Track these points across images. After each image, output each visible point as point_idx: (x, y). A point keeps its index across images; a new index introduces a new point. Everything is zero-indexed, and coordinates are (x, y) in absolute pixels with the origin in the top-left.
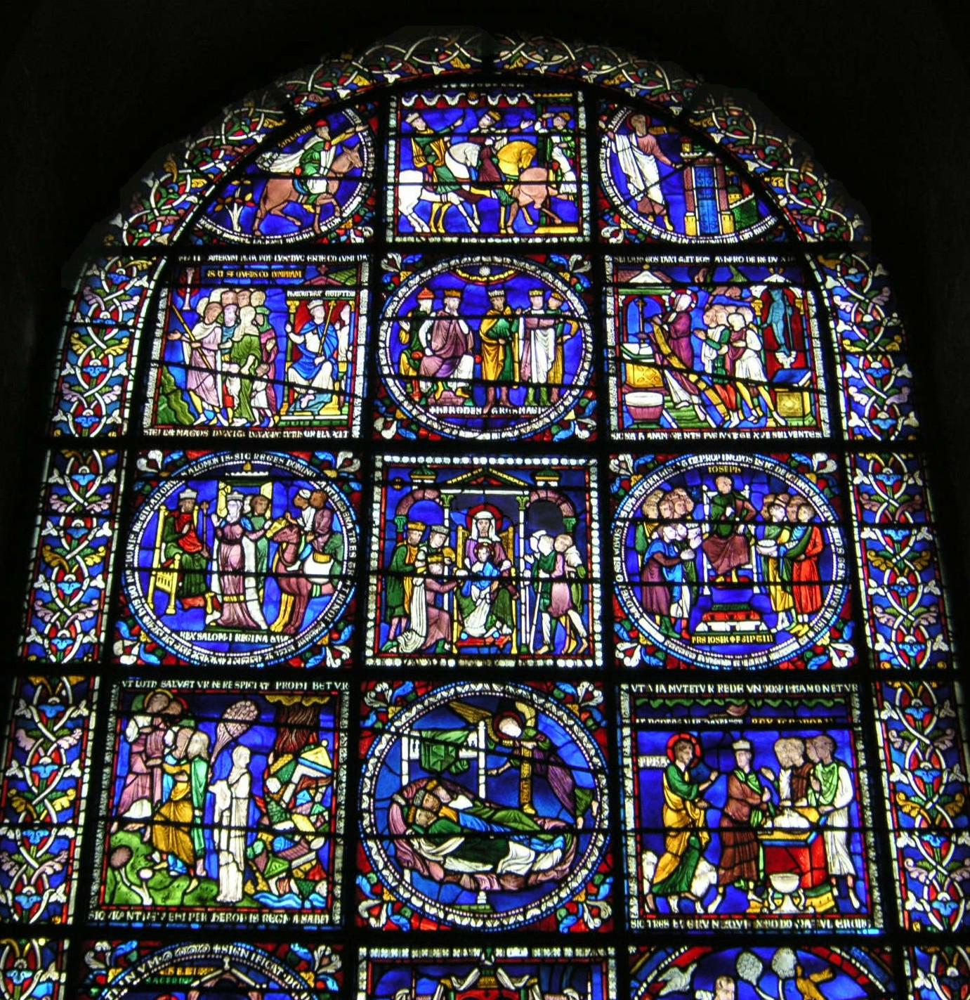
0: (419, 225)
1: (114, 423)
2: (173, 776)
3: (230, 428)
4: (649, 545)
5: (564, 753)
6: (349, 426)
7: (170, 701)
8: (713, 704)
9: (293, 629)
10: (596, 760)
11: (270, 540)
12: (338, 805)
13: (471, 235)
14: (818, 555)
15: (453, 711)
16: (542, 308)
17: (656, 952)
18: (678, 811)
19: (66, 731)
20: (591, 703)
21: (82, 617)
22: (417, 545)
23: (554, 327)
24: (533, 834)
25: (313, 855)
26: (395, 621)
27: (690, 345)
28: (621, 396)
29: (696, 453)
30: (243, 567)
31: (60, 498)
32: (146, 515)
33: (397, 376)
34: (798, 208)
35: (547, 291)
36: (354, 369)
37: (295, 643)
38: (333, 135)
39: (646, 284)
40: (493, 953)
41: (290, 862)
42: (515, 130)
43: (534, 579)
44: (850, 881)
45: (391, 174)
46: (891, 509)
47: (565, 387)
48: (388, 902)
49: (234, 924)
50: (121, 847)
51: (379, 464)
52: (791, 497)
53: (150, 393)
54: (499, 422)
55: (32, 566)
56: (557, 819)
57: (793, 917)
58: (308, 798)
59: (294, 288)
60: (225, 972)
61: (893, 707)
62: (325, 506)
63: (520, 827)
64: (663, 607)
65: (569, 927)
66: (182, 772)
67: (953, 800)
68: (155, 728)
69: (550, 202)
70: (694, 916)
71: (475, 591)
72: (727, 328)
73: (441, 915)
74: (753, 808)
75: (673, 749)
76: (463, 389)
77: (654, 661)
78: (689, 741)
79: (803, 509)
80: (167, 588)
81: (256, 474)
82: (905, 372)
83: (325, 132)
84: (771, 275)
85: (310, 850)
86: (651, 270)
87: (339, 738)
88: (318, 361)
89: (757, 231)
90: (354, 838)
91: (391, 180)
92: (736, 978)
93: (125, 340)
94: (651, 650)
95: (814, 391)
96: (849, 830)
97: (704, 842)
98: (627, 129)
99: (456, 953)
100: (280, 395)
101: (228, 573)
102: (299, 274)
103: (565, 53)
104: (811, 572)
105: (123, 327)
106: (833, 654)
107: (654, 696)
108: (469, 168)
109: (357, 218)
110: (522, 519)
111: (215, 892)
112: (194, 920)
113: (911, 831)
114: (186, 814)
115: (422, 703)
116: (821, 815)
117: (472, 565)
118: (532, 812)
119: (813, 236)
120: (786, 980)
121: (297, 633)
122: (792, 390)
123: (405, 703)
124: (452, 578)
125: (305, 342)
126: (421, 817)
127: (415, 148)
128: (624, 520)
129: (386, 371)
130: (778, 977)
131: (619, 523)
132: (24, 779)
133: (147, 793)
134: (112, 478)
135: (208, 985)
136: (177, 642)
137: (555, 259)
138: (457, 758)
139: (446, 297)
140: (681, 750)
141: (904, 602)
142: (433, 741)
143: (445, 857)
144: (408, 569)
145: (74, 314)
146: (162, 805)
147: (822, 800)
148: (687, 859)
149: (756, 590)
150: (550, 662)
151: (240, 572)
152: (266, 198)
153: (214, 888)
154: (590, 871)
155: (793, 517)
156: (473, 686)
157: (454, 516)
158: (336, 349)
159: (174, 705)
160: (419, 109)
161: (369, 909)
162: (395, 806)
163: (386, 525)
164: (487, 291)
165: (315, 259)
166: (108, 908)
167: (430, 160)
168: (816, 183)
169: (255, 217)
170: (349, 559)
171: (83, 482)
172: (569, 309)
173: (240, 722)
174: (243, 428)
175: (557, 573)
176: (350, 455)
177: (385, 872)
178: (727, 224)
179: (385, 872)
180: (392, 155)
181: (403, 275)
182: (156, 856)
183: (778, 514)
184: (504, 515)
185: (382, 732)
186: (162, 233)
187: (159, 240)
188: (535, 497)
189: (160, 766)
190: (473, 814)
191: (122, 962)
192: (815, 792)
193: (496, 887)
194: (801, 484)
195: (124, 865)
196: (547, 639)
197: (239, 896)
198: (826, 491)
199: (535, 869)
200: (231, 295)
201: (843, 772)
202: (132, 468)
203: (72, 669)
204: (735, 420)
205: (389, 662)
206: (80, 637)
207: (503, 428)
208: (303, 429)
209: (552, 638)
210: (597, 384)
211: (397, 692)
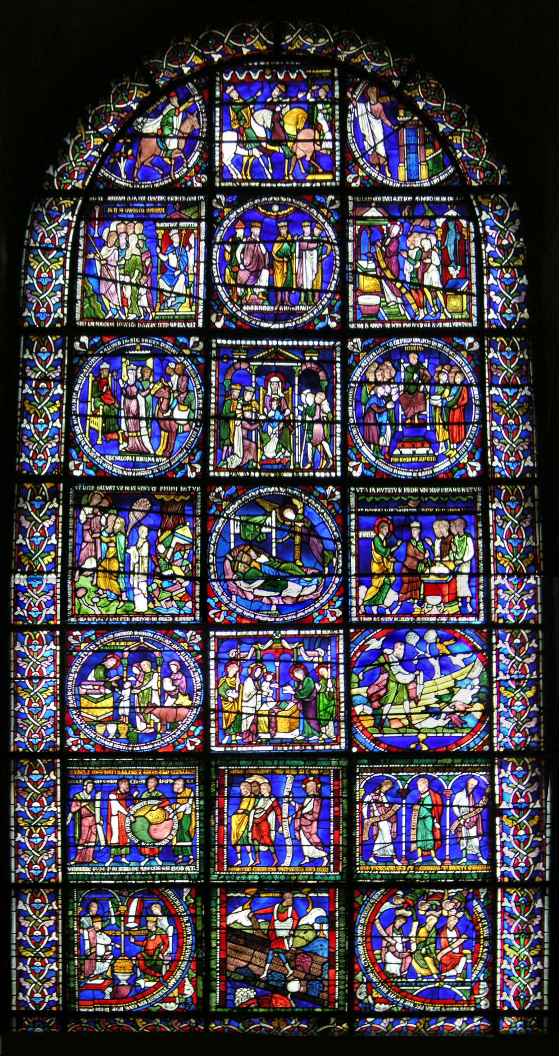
0: (236, 174)
1: (58, 318)
2: (107, 543)
3: (127, 321)
4: (369, 399)
5: (319, 529)
6: (196, 320)
8: (401, 499)
9: (168, 454)
10: (336, 533)
11: (153, 396)
12: (197, 560)
13: (267, 181)
14: (465, 405)
15: (258, 504)
16: (310, 235)
18: (379, 564)
19: (46, 517)
21: (50, 446)
22: (237, 400)
23: (317, 248)
26: (225, 448)
27: (398, 261)
28: (356, 297)
29: (398, 337)
30: (139, 414)
31: (31, 369)
32: (81, 380)
33: (224, 284)
34: (468, 160)
35: (313, 222)
36: (198, 279)
37: (170, 463)
38: (181, 104)
39: (373, 218)
42: (295, 100)
43: (303, 421)
45: (217, 134)
46: (509, 375)
47: (324, 291)
51: (214, 345)
52: (452, 367)
53: (79, 297)
54: (284, 316)
55: (19, 413)
56: (314, 568)
59: (161, 220)
61: (500, 501)
62: (184, 374)
63: (294, 573)
64: (376, 439)
66: (111, 541)
67: (528, 557)
68: (95, 515)
69: (316, 155)
71: (270, 429)
72: (420, 249)
74: (420, 561)
75: (378, 527)
76: (263, 293)
77: (369, 473)
78: (386, 522)
79: (458, 375)
80: (97, 428)
81: (143, 352)
82: (524, 281)
83: (175, 101)
84: (448, 210)
86: (376, 207)
88: (177, 273)
89: (442, 178)
90: (205, 580)
91: (217, 139)
93: (61, 259)
94: (368, 466)
95: (470, 294)
98: (365, 99)
100: (155, 298)
101: (130, 418)
102: (163, 210)
103: (326, 37)
104: (460, 416)
105: (59, 249)
106: (469, 468)
107: (368, 495)
108: (266, 129)
109: (197, 169)
110: (297, 382)
113: (503, 575)
114: (115, 566)
117: (268, 412)
118: (300, 564)
119: (476, 181)
121: (170, 456)
122: (457, 293)
123: (231, 499)
124: (257, 421)
125: (168, 260)
126: (241, 567)
127: (232, 113)
128: (355, 382)
129: (217, 280)
131: (352, 385)
132: (26, 545)
134: (60, 355)
136: (104, 462)
137: (318, 198)
138: (261, 533)
139: (252, 227)
141: (511, 435)
142: (247, 522)
144: (232, 415)
145: (29, 240)
149: (428, 428)
150: (311, 474)
151: (137, 417)
152: (140, 153)
155: (452, 380)
157: (259, 380)
158: (187, 265)
159: (105, 501)
160: (234, 82)
162: (227, 562)
163: (220, 386)
164: (277, 222)
165: (172, 199)
167: (242, 123)
168: (481, 141)
169: (135, 168)
170: (199, 409)
171: (44, 358)
172: (326, 236)
173: (142, 511)
174: (135, 321)
175: (316, 417)
176: (197, 339)
178: (424, 172)
180: (217, 119)
181: (226, 211)
182: (100, 592)
183: (443, 378)
184: (287, 381)
186: (78, 180)
187: (77, 185)
188: (304, 368)
189: (100, 538)
190: (269, 566)
194: (458, 358)
195: (84, 596)
196: (310, 459)
198: (472, 363)
200: (122, 226)
201: (469, 540)
202: (71, 348)
203: (47, 478)
204: (422, 314)
205: (222, 474)
206: (50, 459)
207: (285, 321)
208: (169, 321)
209: (313, 459)
210: (342, 290)
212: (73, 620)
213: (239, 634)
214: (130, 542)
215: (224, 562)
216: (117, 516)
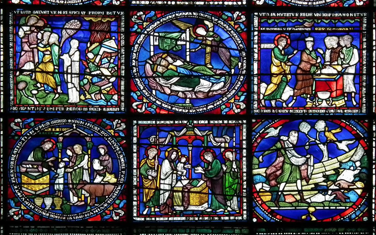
2: (43, 52)
7: (38, 20)
10: (241, 45)
12: (121, 64)
15: (174, 24)
17: (264, 122)
18: (278, 66)
20: (240, 21)
24: (212, 76)
25: (111, 84)
40: (193, 122)
41: (100, 87)
44: (353, 95)
48: (145, 103)
49: (76, 111)
50: (22, 81)
56: (222, 70)
57: (326, 109)
58: (107, 61)
60: (74, 130)
63: (205, 73)
65: (226, 112)
66: (47, 51)
68: (33, 31)
70: (282, 108)
73: (170, 108)
74: (312, 65)
75: (277, 40)
85: (110, 82)
87: (120, 36)
90: (129, 77)
92: (298, 131)
96: (355, 75)
97: (289, 79)
99: (176, 122)
107: (270, 18)
111: (67, 99)
112: (58, 110)
114: (50, 68)
115: (159, 21)
116: (343, 68)
120: (319, 132)
123: (151, 21)
126: (160, 69)
130: (317, 131)
133: (32, 59)
135: (67, 135)
138: (176, 45)
140: (281, 41)
142: (164, 37)
143: (171, 85)
146: (39, 64)
147: (344, 62)
148: (281, 85)
153: (66, 97)
154: (236, 90)
156: (184, 13)
159: (40, 21)
161: (137, 106)
162: (148, 66)
166: (19, 106)
173: (73, 29)
177: (144, 91)
179: (144, 91)
182: (39, 85)
185: (140, 34)
189: (36, 48)
191: (28, 126)
192: (341, 59)
193: (194, 97)
195: (24, 89)
197: (78, 100)
199: (212, 89)
211: (147, 16)
212: (14, 108)
213: (158, 122)
214: (64, 49)
215: (145, 65)
216: (52, 32)
